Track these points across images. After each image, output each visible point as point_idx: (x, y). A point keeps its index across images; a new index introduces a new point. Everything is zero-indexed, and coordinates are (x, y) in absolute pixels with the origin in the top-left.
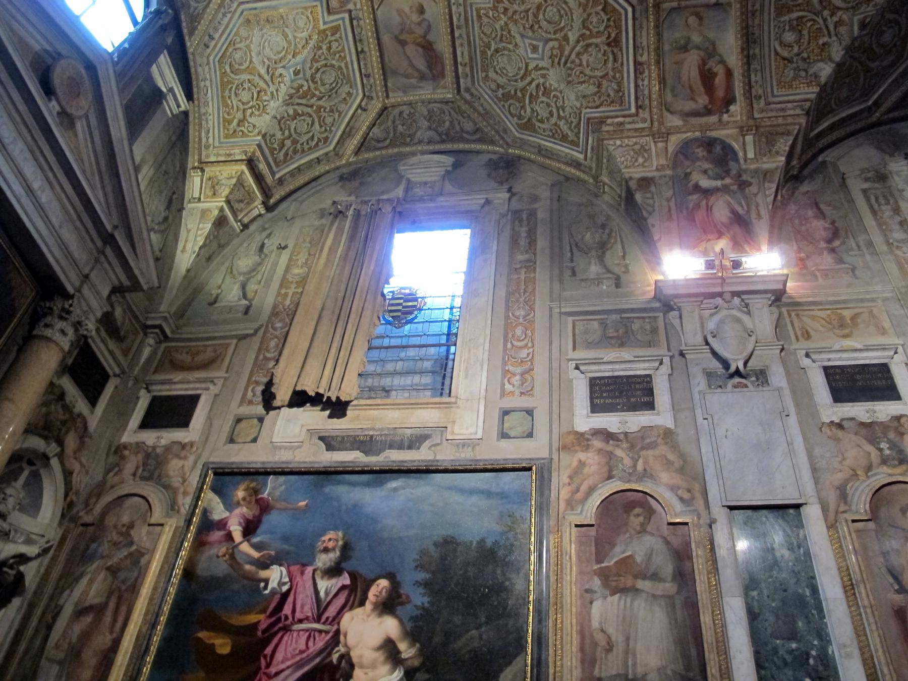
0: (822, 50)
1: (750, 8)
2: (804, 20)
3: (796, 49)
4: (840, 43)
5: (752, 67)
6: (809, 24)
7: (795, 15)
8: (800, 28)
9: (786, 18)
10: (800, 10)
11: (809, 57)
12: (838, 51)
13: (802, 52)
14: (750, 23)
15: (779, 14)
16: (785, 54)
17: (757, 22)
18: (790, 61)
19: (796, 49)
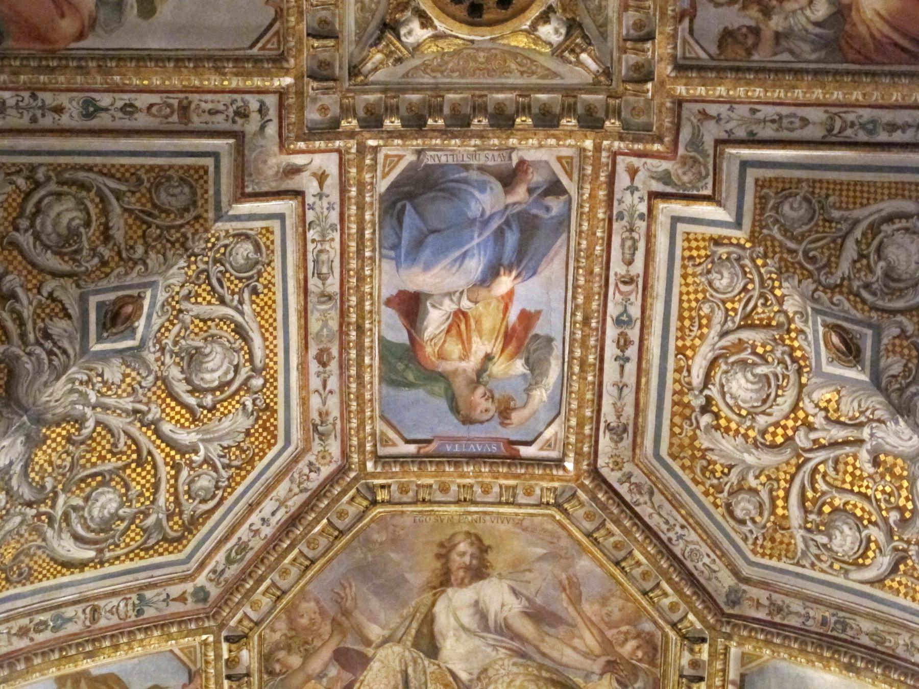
0: (890, 471)
1: (762, 615)
2: (810, 494)
3: (876, 534)
4: (879, 421)
5: (900, 651)
6: (821, 486)
7: (795, 514)
8: (827, 509)
9: (799, 534)
10: (786, 499)
11: (901, 510)
12: (897, 434)
13: (886, 520)
14: (794, 621)
15: (788, 552)
16: (885, 562)
17: (796, 606)
18: (901, 558)
19: (876, 534)
